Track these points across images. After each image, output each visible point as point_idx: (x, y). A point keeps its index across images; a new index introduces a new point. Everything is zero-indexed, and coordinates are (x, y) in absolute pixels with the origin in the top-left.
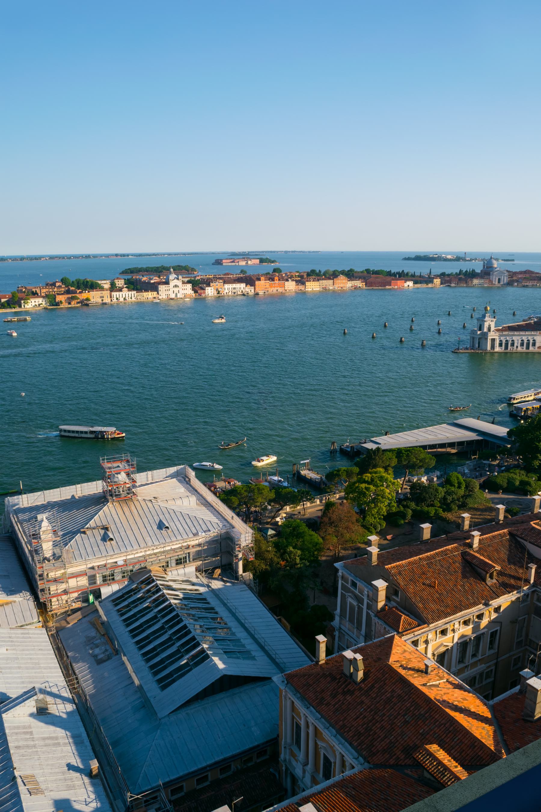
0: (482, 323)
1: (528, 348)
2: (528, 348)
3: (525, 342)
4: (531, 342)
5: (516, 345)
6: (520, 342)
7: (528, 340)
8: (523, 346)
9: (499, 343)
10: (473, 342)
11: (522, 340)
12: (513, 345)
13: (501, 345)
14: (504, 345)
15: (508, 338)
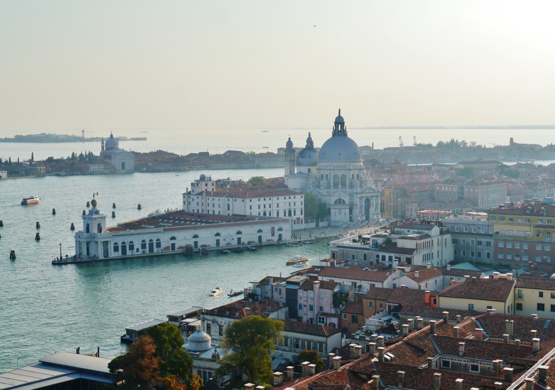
0: (89, 222)
1: (151, 250)
2: (151, 250)
3: (147, 242)
4: (155, 242)
5: (135, 248)
6: (140, 242)
7: (151, 240)
8: (145, 248)
9: (114, 247)
10: (80, 248)
11: (143, 241)
12: (132, 248)
13: (116, 249)
14: (120, 248)
15: (126, 241)
